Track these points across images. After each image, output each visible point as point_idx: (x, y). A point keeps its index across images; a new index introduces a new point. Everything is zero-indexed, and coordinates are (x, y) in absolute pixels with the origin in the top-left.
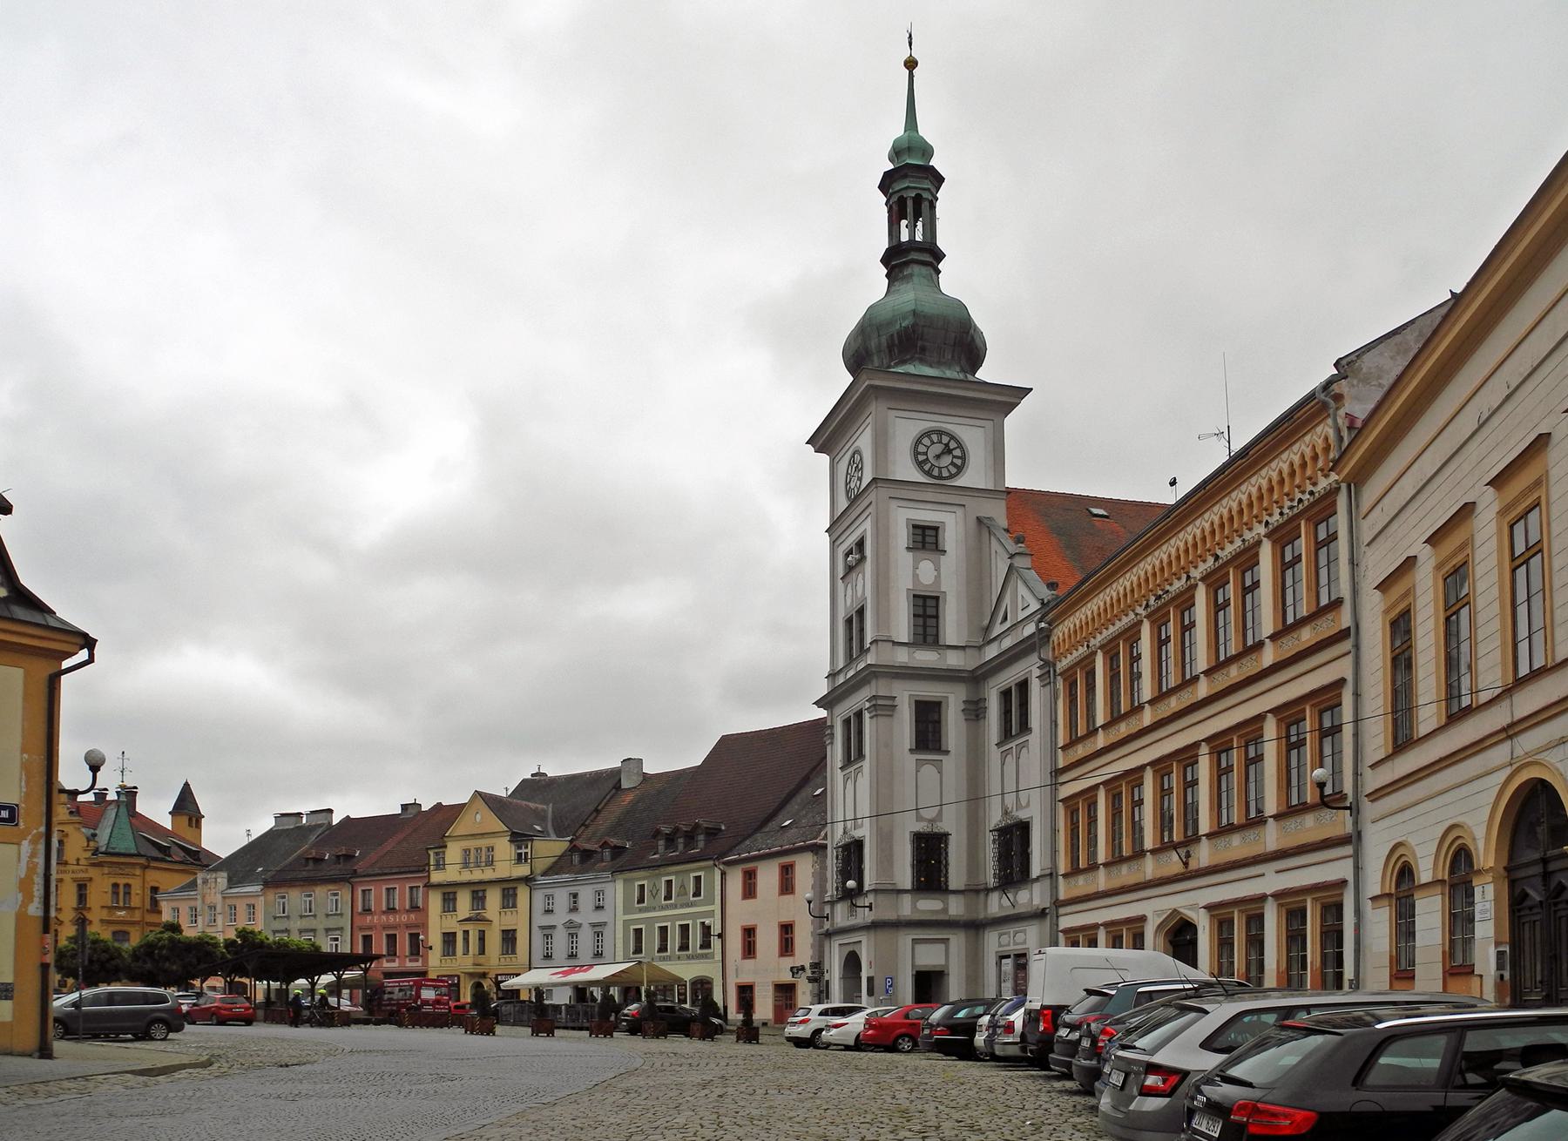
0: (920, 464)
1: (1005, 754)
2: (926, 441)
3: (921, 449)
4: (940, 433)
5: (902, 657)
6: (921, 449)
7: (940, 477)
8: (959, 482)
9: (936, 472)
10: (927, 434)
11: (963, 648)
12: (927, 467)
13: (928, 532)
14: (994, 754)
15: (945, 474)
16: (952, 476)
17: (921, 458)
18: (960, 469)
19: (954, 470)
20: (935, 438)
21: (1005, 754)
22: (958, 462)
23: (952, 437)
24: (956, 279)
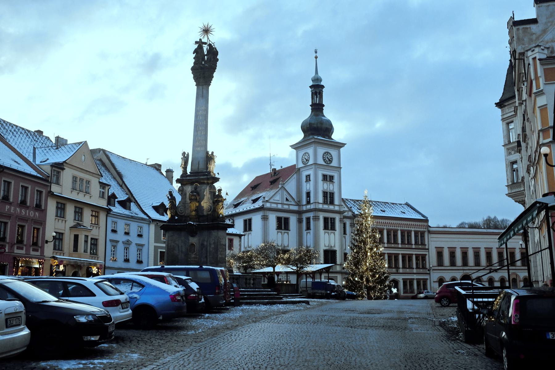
1: (307, 233)
8: (331, 165)
10: (325, 153)
14: (305, 232)
21: (307, 233)
24: (328, 114)
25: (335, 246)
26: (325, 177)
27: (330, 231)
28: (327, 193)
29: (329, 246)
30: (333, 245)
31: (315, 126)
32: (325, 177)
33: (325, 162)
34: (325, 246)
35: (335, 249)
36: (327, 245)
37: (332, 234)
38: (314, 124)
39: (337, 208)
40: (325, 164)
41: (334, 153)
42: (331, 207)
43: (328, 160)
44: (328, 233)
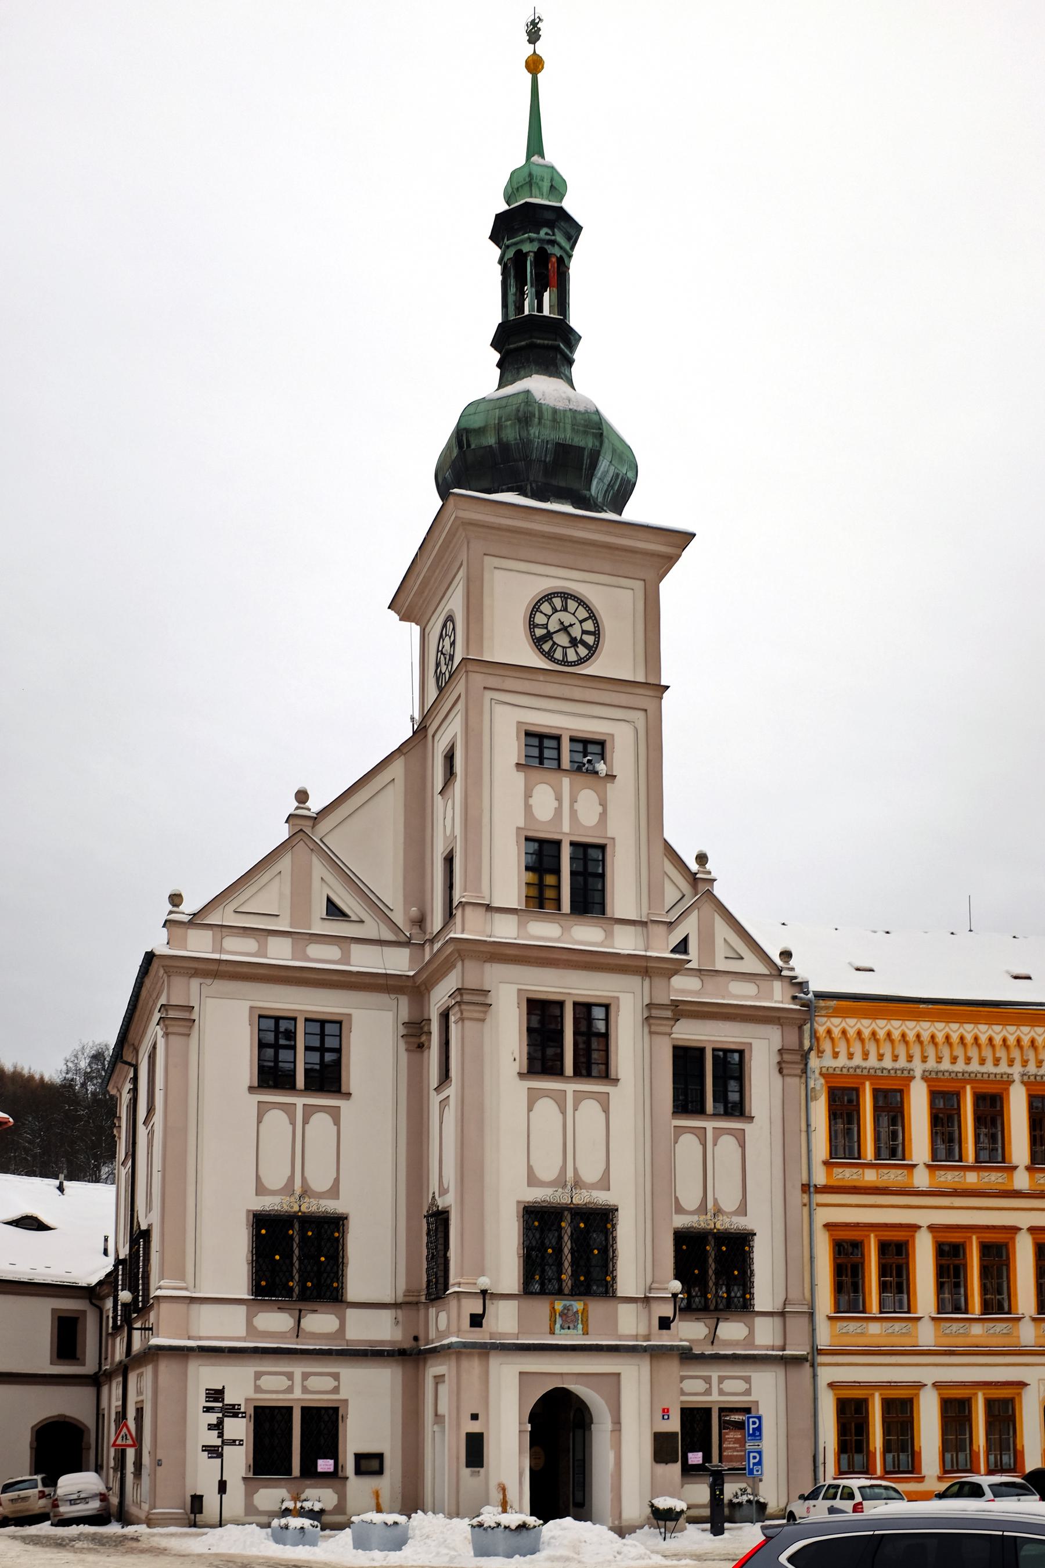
0: (538, 642)
2: (546, 608)
3: (540, 619)
4: (565, 596)
5: (505, 930)
6: (540, 619)
7: (565, 662)
9: (558, 655)
10: (548, 598)
11: (643, 924)
12: (546, 647)
13: (547, 743)
15: (572, 656)
16: (581, 661)
17: (539, 632)
18: (593, 650)
19: (583, 651)
20: (558, 602)
22: (590, 639)
23: (581, 602)
25: (604, 1183)
26: (540, 748)
27: (570, 1088)
28: (558, 844)
29: (560, 1182)
30: (590, 1173)
31: (491, 440)
32: (540, 748)
33: (549, 656)
34: (532, 1180)
35: (601, 1198)
36: (547, 1171)
37: (590, 1109)
38: (481, 431)
39: (626, 943)
40: (539, 662)
41: (612, 600)
42: (586, 935)
43: (564, 639)
44: (560, 1100)
